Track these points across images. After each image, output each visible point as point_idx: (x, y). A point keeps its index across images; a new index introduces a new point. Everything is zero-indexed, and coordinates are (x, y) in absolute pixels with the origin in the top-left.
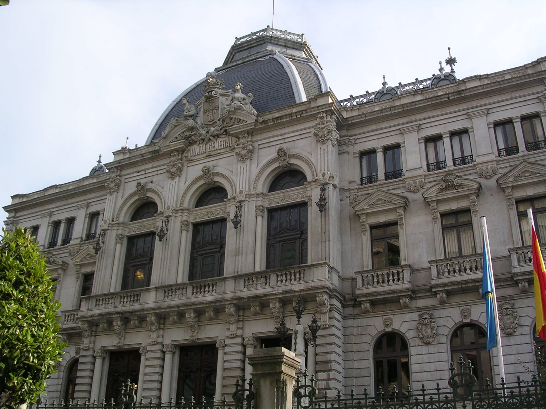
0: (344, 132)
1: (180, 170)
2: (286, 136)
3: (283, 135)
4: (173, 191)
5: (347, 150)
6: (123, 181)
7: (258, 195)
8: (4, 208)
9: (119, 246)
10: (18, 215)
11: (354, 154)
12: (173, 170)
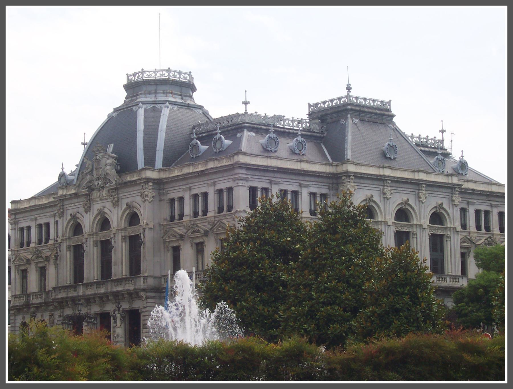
1: (90, 207)
2: (132, 193)
3: (130, 192)
4: (88, 222)
6: (65, 209)
7: (122, 230)
9: (68, 252)
10: (17, 216)
12: (86, 207)
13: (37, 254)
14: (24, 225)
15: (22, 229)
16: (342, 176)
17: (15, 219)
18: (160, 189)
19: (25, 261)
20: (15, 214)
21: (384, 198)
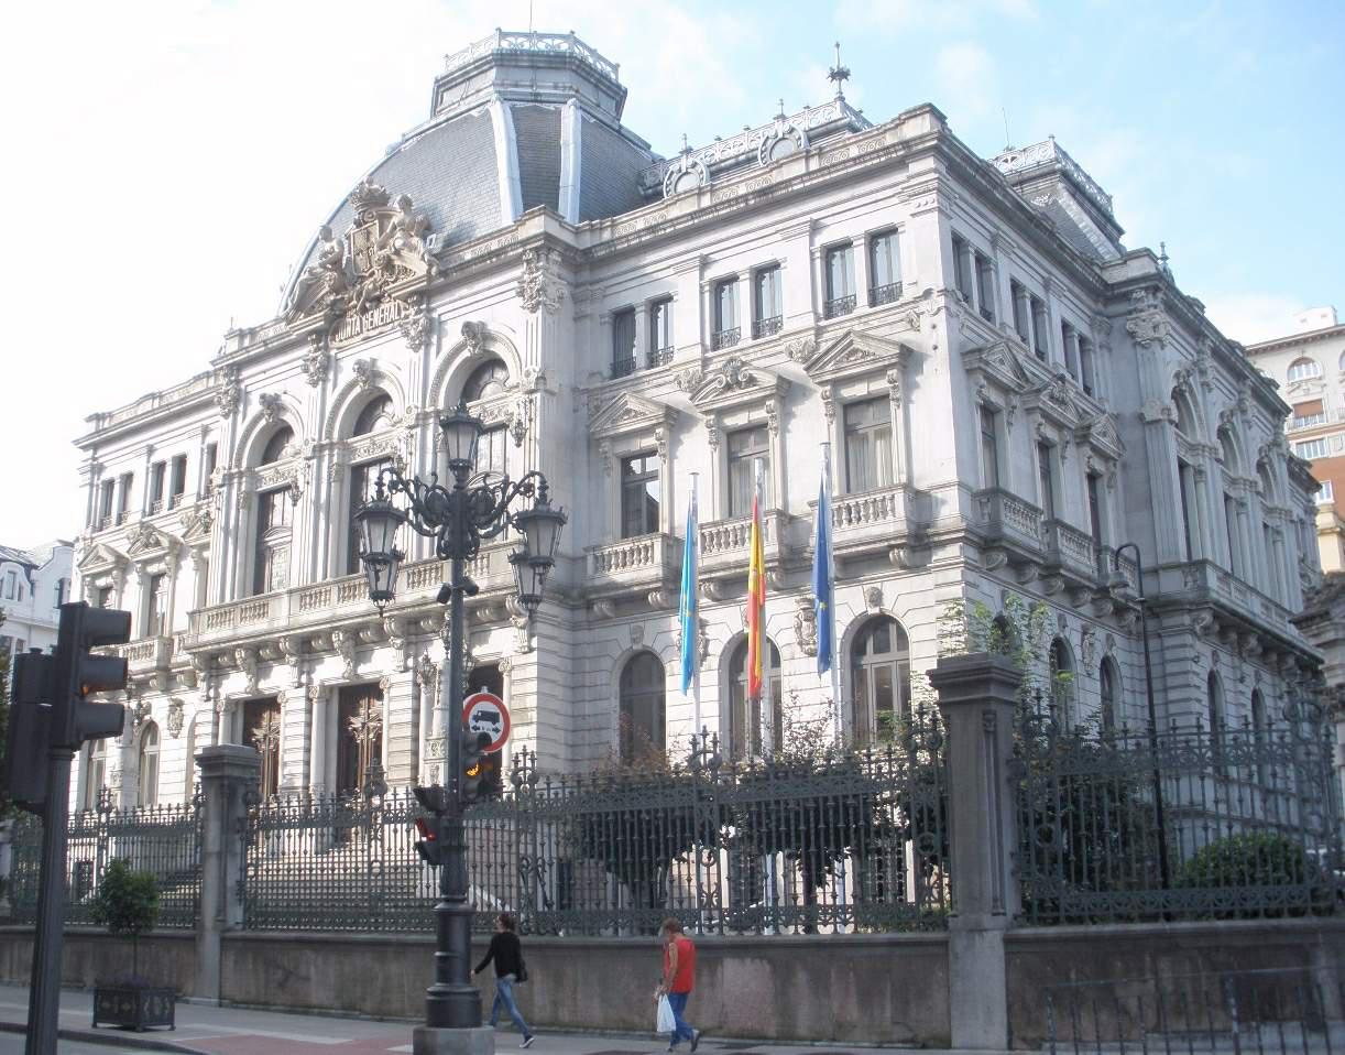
0: (586, 276)
5: (589, 311)
8: (76, 442)
10: (101, 452)
11: (602, 317)
13: (148, 536)
14: (113, 472)
15: (110, 484)
16: (1132, 292)
17: (94, 459)
18: (577, 286)
19: (111, 559)
20: (96, 446)
21: (1203, 384)
